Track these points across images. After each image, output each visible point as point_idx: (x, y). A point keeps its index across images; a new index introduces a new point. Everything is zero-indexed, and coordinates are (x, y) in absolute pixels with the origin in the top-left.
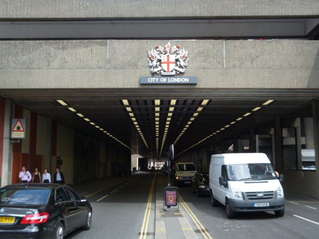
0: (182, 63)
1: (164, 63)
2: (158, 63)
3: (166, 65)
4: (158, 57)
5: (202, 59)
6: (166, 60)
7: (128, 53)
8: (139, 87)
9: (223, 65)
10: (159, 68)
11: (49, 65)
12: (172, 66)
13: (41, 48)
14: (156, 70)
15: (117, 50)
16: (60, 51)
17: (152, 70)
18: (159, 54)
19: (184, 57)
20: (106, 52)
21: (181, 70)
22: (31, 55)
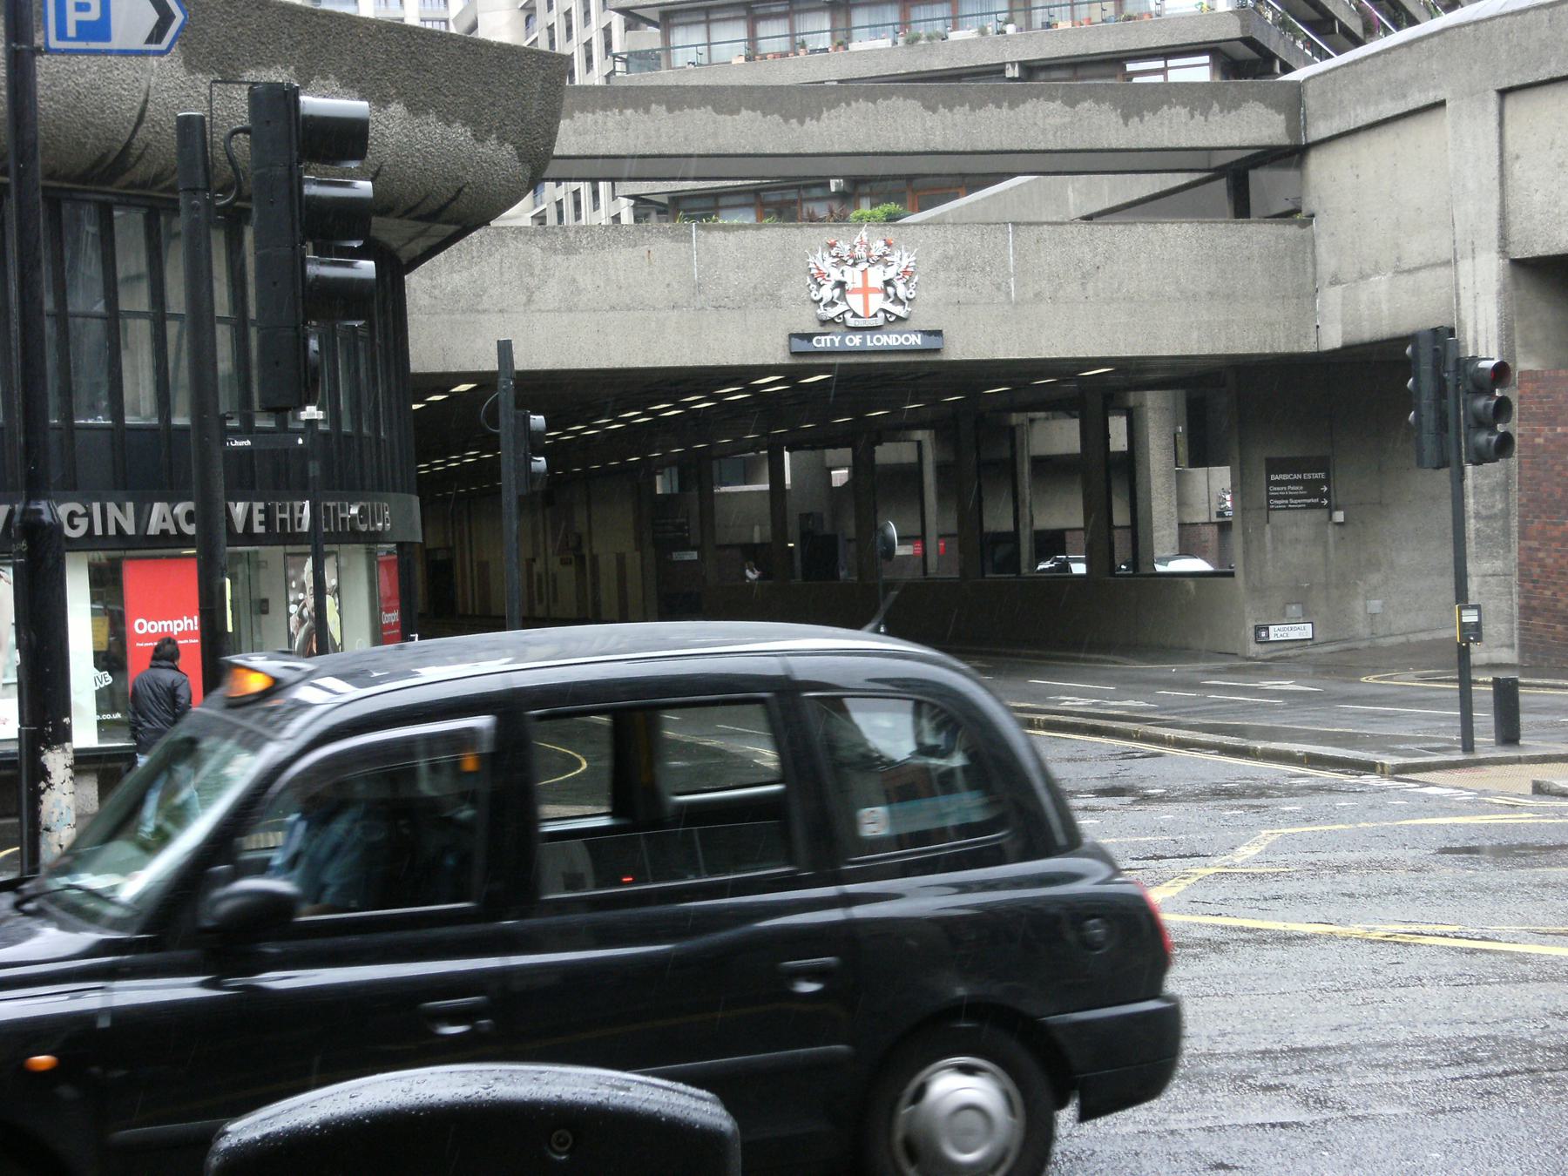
0: (902, 292)
1: (855, 291)
2: (837, 291)
3: (860, 297)
4: (836, 275)
5: (954, 277)
6: (859, 284)
7: (751, 263)
8: (786, 362)
9: (1008, 294)
10: (841, 307)
11: (529, 301)
12: (877, 302)
13: (505, 250)
14: (832, 312)
15: (721, 253)
16: (560, 258)
17: (821, 311)
18: (836, 265)
19: (905, 272)
20: (689, 259)
21: (899, 310)
22: (475, 270)
